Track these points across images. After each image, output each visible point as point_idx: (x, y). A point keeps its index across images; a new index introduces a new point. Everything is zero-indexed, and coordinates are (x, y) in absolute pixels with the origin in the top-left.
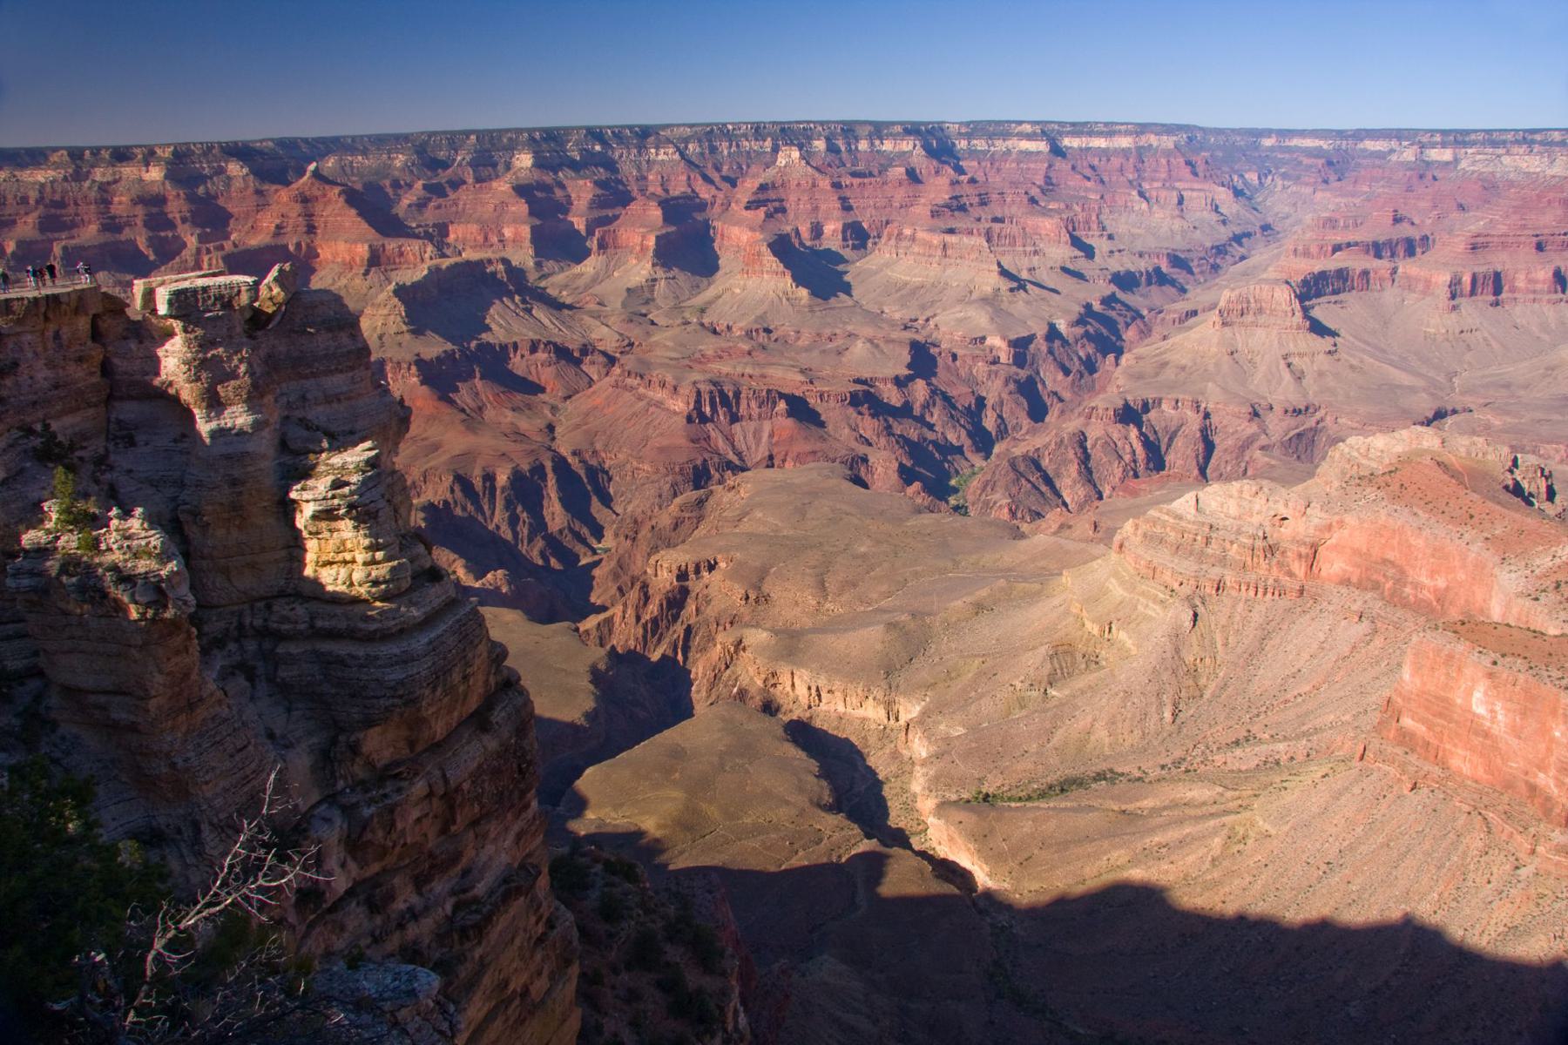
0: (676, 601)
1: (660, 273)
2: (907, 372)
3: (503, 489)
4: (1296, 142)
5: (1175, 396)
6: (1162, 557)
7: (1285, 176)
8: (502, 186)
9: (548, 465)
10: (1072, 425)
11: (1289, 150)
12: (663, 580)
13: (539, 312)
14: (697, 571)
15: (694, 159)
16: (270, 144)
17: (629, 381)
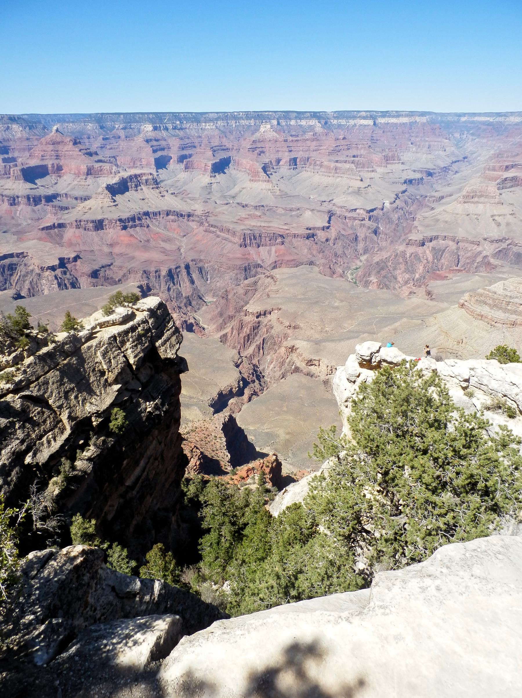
0: (256, 328)
1: (213, 180)
2: (328, 225)
3: (164, 277)
4: (476, 119)
5: (444, 234)
6: (485, 310)
7: (472, 134)
8: (139, 140)
9: (183, 266)
10: (401, 248)
11: (473, 122)
12: (250, 319)
13: (169, 198)
14: (265, 314)
15: (222, 129)
16: (26, 117)
17: (212, 229)
